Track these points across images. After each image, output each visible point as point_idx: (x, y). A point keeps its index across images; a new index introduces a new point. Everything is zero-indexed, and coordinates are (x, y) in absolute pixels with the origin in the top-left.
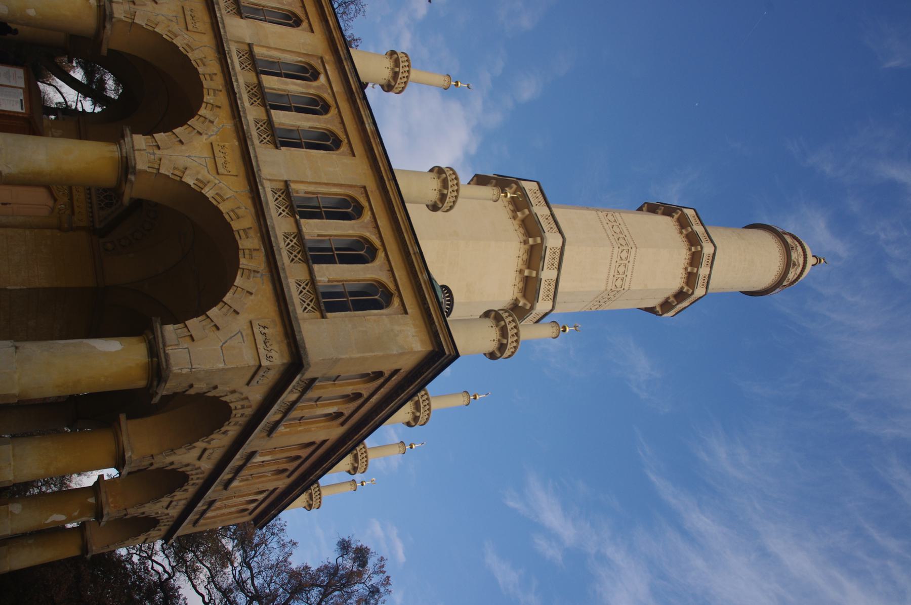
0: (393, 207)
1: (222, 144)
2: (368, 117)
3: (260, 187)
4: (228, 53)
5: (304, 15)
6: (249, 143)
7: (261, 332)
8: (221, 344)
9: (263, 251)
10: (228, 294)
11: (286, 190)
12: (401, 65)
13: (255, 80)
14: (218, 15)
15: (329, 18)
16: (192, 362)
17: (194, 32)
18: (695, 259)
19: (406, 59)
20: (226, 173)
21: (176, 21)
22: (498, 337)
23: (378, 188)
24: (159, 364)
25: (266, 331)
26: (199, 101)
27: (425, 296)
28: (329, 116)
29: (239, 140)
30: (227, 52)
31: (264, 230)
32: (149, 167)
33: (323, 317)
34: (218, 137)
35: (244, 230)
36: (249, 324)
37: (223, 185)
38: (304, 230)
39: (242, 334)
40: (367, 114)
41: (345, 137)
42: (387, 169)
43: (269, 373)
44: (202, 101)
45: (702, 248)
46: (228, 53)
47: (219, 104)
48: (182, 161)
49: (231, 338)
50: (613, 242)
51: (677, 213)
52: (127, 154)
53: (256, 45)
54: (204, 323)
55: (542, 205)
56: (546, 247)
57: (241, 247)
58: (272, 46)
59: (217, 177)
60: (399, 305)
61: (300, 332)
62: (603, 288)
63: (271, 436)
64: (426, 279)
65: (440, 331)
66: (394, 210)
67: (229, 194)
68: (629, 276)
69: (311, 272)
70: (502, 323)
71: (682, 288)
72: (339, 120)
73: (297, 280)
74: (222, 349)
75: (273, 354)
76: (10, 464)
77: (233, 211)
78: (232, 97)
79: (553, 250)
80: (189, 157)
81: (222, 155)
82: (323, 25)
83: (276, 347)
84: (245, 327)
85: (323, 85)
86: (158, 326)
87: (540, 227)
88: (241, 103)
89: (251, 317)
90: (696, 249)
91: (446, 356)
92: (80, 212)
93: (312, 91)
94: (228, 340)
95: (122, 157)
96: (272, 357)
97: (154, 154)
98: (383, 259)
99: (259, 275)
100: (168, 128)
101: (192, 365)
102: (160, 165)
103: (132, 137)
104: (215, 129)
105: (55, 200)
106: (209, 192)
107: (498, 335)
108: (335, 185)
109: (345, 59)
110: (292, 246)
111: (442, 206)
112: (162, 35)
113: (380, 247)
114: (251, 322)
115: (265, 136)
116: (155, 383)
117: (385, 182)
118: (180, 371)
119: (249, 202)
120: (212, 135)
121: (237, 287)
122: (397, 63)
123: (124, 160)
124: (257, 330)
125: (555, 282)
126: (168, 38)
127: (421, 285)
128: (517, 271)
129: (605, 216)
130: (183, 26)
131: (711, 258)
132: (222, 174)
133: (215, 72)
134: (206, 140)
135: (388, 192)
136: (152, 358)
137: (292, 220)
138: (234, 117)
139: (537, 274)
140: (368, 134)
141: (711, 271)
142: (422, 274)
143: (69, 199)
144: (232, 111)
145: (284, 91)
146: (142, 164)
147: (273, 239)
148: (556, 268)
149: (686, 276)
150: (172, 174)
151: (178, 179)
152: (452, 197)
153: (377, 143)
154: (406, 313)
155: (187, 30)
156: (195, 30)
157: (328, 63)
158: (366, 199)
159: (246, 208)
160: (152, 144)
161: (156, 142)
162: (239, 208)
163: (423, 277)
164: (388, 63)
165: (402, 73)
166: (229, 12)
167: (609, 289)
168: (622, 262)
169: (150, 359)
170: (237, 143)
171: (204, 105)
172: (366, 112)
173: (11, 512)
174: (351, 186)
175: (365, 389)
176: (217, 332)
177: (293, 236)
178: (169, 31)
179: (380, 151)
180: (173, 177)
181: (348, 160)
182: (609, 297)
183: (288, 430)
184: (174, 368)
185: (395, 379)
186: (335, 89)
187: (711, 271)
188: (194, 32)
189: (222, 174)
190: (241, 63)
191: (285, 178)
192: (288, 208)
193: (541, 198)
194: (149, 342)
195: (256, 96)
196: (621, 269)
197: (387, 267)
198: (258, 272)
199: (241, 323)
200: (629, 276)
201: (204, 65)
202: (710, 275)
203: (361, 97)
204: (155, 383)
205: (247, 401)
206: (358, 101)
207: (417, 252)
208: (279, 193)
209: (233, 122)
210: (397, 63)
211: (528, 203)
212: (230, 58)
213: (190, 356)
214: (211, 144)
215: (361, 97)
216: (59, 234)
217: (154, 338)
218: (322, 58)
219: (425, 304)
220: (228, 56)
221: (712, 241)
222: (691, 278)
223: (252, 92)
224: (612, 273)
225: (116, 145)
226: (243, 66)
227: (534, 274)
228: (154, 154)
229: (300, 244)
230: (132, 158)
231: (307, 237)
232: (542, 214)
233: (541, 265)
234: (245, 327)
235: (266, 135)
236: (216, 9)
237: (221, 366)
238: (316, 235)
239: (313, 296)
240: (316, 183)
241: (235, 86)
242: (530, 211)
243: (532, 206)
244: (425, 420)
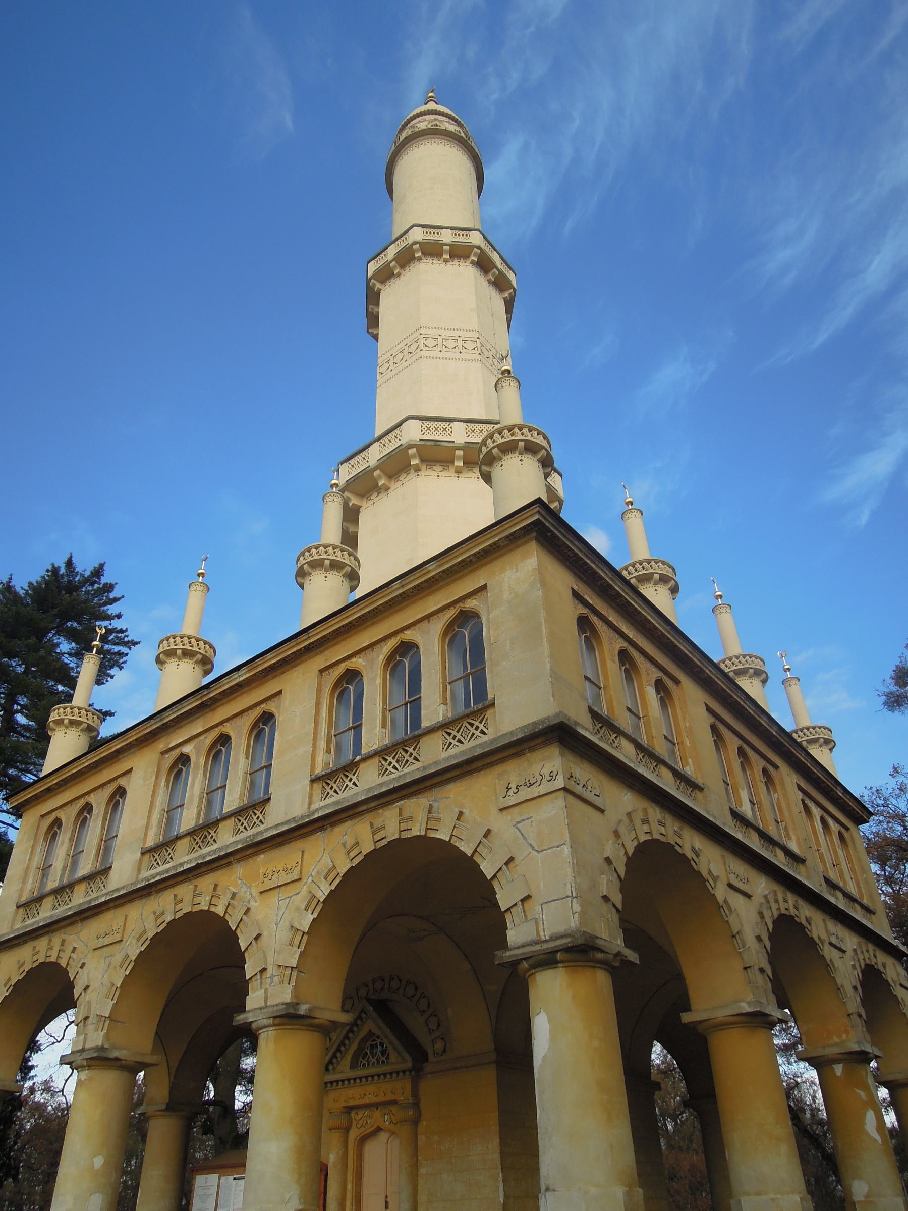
0: (343, 626)
1: (262, 877)
2: (231, 679)
3: (316, 816)
4: (149, 880)
5: (112, 783)
6: (260, 838)
7: (515, 793)
8: (534, 852)
9: (402, 802)
10: (462, 848)
11: (324, 779)
12: (173, 647)
13: (186, 840)
14: (103, 899)
15: (113, 749)
16: (562, 897)
17: (124, 931)
18: (432, 250)
19: (165, 642)
20: (299, 867)
21: (110, 957)
22: (517, 455)
23: (321, 652)
24: (567, 949)
25: (513, 786)
26: (208, 915)
27: (459, 563)
28: (232, 734)
29: (257, 853)
30: (147, 883)
31: (373, 804)
32: (289, 984)
33: (493, 705)
34: (253, 884)
35: (374, 833)
36: (505, 812)
37: (315, 870)
38: (375, 747)
39: (518, 823)
40: (228, 680)
41: (258, 708)
42: (295, 643)
43: (578, 776)
44: (208, 911)
45: (415, 243)
46: (149, 880)
47: (212, 886)
48: (284, 934)
49: (525, 838)
50: (414, 358)
51: (374, 285)
52: (270, 1018)
53: (144, 843)
54: (503, 882)
55: (367, 455)
56: (420, 440)
57: (397, 836)
58: (145, 822)
59: (304, 880)
60: (475, 599)
61: (511, 733)
62: (479, 365)
63: (702, 786)
64: (436, 565)
65: (507, 533)
66: (346, 624)
67: (326, 862)
68: (460, 333)
69: (431, 730)
70: (495, 451)
71: (473, 263)
72: (237, 719)
73: (443, 749)
74: (542, 851)
75: (546, 772)
76: (773, 1200)
77: (348, 853)
78: (204, 869)
79: (424, 431)
80: (277, 924)
81: (276, 875)
83: (536, 768)
84: (509, 817)
85: (195, 747)
86: (508, 953)
87: (394, 452)
88: (210, 855)
89: (494, 810)
90: (417, 251)
91: (541, 518)
92: (392, 1092)
93: (202, 761)
94: (528, 843)
95: (275, 1025)
96: (552, 772)
97: (272, 976)
98: (414, 632)
99: (435, 805)
100: (238, 959)
101: (568, 897)
102: (286, 967)
103: (249, 1011)
104: (244, 889)
105: (379, 1129)
106: (323, 890)
107: (513, 456)
108: (317, 712)
109: (161, 720)
110: (398, 761)
111: (350, 566)
112: (126, 975)
113: (398, 638)
114: (501, 810)
115: (255, 818)
116: (600, 956)
117: (312, 643)
118: (576, 915)
119: (338, 829)
120: (251, 894)
121: (452, 835)
122: (170, 653)
123: (278, 1021)
124: (512, 800)
125: (469, 424)
126: (130, 967)
127: (444, 571)
128: (458, 477)
129: (383, 375)
130: (117, 946)
131: (429, 230)
132: (301, 873)
133: (172, 896)
134: (256, 902)
135: (324, 636)
136: (557, 962)
137: (362, 766)
138: (229, 864)
139: (459, 448)
140: (252, 676)
141: (447, 228)
142: (429, 572)
143: (377, 1109)
144: (221, 867)
145: (201, 799)
146: (283, 995)
147: (384, 789)
148: (449, 425)
149: (456, 260)
150: (298, 948)
151: (305, 937)
152: (335, 553)
153: (262, 661)
154: (484, 587)
155: (121, 941)
156: (121, 931)
157: (169, 744)
158: (336, 667)
159: (346, 834)
160: (259, 981)
161: (256, 974)
162: (344, 845)
163: (434, 570)
164: (172, 665)
165: (183, 645)
166: (104, 886)
167: (479, 357)
168: (440, 344)
169: (560, 965)
170: (262, 856)
171: (213, 909)
172: (225, 682)
173: (867, 1196)
174: (319, 691)
175: (611, 645)
176: (517, 861)
177: (383, 763)
178: (121, 966)
179: (275, 654)
180: (303, 946)
181: (286, 698)
182: (491, 357)
183: (690, 760)
184: (573, 925)
185: (590, 598)
186: (200, 730)
187: (447, 228)
188: (124, 931)
189: (301, 873)
190: (165, 862)
191: (308, 782)
192: (347, 773)
193: (359, 457)
194: (535, 968)
195: (206, 837)
196: (450, 344)
197: (424, 624)
198: (431, 806)
199: (502, 825)
200: (460, 333)
201: (163, 913)
202: (452, 228)
203: (206, 692)
204: (600, 956)
205: (633, 815)
206: (212, 695)
207: (401, 582)
208: (328, 789)
209: (235, 865)
210: (170, 653)
211: (365, 473)
212: (154, 878)
213: (554, 900)
214: (261, 893)
216: (424, 1123)
217: (525, 959)
218: (163, 753)
219: (471, 561)
220: (152, 881)
221: (406, 232)
222: (458, 253)
223: (200, 843)
224: (458, 355)
225: (259, 1034)
226: (168, 859)
227: (460, 453)
228: (272, 976)
229: (395, 750)
230: (275, 1008)
231: (387, 741)
232: (379, 453)
233: (446, 444)
234: (509, 817)
235: (253, 816)
236: (97, 902)
237: (566, 850)
238: (384, 730)
239: (465, 724)
240: (315, 739)
241: (189, 866)
242: (375, 469)
244: (665, 566)
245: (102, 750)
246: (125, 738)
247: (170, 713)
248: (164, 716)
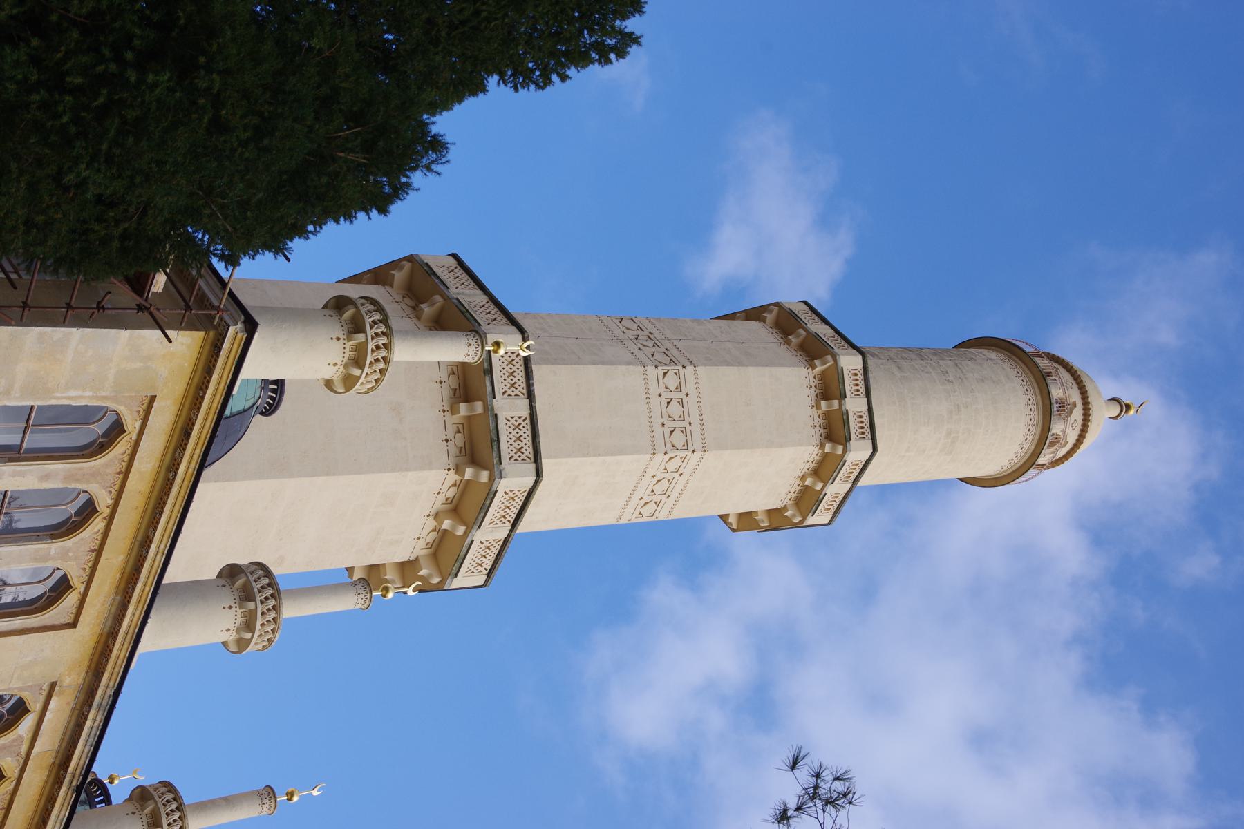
2: (59, 821)
40: (61, 817)
82: (114, 601)
109: (100, 706)
172: (63, 813)
206: (63, 789)
215: (74, 784)
243: (479, 527)
245: (147, 589)
246: (129, 637)
247: (96, 723)
248: (101, 713)
